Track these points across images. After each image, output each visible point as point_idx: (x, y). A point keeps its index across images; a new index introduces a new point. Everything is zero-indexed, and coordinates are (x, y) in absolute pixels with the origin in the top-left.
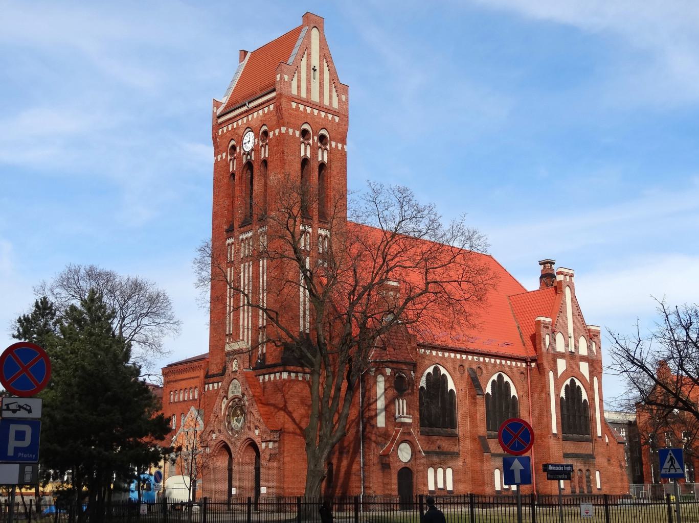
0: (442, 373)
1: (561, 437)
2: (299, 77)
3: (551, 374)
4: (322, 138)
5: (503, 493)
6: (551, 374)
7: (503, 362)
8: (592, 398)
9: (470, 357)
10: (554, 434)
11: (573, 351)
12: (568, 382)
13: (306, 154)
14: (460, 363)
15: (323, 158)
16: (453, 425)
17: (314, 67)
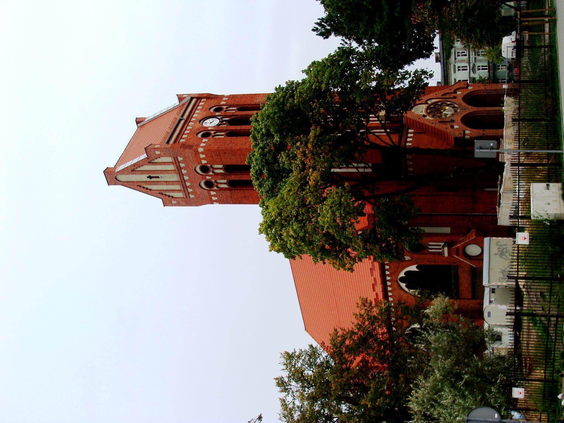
2: (166, 191)
4: (205, 169)
13: (224, 183)
17: (148, 177)
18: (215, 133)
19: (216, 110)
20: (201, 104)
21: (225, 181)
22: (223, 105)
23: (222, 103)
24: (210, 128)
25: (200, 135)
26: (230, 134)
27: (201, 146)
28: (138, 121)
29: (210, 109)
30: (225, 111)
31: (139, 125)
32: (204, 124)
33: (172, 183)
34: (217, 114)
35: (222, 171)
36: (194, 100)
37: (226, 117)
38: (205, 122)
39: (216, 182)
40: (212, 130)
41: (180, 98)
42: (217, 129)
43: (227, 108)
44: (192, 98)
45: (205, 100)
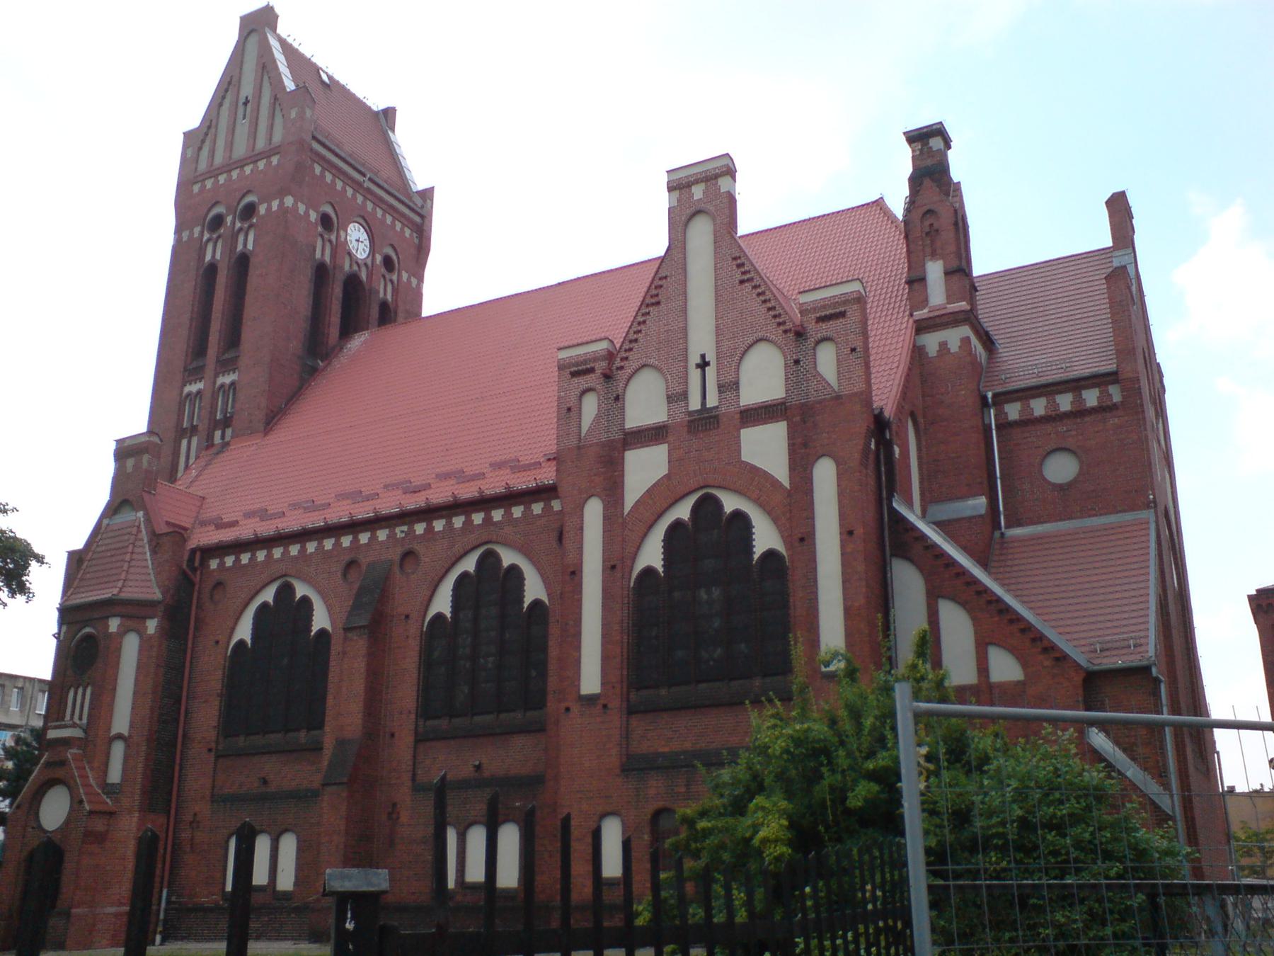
0: (299, 595)
1: (615, 704)
3: (594, 511)
5: (459, 898)
6: (594, 511)
7: (497, 515)
8: (803, 538)
9: (382, 535)
10: (591, 700)
11: (712, 401)
12: (683, 511)
14: (347, 558)
15: (245, 245)
16: (316, 722)
18: (330, 241)
19: (388, 262)
20: (407, 232)
21: (218, 256)
22: (399, 276)
23: (405, 276)
24: (342, 233)
25: (328, 209)
26: (321, 273)
27: (300, 204)
28: (389, 114)
29: (392, 246)
30: (384, 277)
31: (381, 116)
32: (357, 225)
33: (230, 145)
34: (379, 258)
35: (240, 247)
36: (417, 219)
37: (370, 275)
38: (362, 230)
39: (219, 237)
40: (338, 237)
41: (427, 194)
42: (340, 249)
43: (392, 281)
44: (422, 217)
45: (416, 241)
